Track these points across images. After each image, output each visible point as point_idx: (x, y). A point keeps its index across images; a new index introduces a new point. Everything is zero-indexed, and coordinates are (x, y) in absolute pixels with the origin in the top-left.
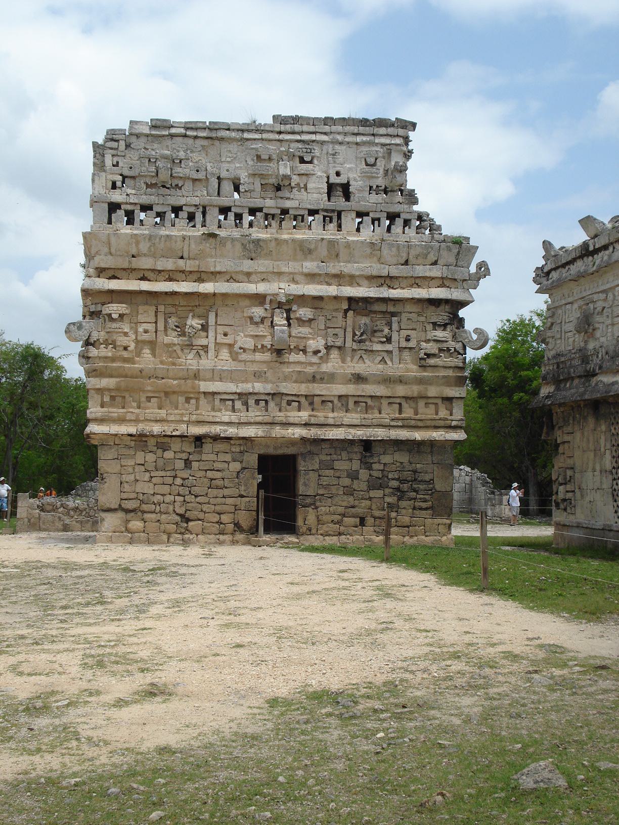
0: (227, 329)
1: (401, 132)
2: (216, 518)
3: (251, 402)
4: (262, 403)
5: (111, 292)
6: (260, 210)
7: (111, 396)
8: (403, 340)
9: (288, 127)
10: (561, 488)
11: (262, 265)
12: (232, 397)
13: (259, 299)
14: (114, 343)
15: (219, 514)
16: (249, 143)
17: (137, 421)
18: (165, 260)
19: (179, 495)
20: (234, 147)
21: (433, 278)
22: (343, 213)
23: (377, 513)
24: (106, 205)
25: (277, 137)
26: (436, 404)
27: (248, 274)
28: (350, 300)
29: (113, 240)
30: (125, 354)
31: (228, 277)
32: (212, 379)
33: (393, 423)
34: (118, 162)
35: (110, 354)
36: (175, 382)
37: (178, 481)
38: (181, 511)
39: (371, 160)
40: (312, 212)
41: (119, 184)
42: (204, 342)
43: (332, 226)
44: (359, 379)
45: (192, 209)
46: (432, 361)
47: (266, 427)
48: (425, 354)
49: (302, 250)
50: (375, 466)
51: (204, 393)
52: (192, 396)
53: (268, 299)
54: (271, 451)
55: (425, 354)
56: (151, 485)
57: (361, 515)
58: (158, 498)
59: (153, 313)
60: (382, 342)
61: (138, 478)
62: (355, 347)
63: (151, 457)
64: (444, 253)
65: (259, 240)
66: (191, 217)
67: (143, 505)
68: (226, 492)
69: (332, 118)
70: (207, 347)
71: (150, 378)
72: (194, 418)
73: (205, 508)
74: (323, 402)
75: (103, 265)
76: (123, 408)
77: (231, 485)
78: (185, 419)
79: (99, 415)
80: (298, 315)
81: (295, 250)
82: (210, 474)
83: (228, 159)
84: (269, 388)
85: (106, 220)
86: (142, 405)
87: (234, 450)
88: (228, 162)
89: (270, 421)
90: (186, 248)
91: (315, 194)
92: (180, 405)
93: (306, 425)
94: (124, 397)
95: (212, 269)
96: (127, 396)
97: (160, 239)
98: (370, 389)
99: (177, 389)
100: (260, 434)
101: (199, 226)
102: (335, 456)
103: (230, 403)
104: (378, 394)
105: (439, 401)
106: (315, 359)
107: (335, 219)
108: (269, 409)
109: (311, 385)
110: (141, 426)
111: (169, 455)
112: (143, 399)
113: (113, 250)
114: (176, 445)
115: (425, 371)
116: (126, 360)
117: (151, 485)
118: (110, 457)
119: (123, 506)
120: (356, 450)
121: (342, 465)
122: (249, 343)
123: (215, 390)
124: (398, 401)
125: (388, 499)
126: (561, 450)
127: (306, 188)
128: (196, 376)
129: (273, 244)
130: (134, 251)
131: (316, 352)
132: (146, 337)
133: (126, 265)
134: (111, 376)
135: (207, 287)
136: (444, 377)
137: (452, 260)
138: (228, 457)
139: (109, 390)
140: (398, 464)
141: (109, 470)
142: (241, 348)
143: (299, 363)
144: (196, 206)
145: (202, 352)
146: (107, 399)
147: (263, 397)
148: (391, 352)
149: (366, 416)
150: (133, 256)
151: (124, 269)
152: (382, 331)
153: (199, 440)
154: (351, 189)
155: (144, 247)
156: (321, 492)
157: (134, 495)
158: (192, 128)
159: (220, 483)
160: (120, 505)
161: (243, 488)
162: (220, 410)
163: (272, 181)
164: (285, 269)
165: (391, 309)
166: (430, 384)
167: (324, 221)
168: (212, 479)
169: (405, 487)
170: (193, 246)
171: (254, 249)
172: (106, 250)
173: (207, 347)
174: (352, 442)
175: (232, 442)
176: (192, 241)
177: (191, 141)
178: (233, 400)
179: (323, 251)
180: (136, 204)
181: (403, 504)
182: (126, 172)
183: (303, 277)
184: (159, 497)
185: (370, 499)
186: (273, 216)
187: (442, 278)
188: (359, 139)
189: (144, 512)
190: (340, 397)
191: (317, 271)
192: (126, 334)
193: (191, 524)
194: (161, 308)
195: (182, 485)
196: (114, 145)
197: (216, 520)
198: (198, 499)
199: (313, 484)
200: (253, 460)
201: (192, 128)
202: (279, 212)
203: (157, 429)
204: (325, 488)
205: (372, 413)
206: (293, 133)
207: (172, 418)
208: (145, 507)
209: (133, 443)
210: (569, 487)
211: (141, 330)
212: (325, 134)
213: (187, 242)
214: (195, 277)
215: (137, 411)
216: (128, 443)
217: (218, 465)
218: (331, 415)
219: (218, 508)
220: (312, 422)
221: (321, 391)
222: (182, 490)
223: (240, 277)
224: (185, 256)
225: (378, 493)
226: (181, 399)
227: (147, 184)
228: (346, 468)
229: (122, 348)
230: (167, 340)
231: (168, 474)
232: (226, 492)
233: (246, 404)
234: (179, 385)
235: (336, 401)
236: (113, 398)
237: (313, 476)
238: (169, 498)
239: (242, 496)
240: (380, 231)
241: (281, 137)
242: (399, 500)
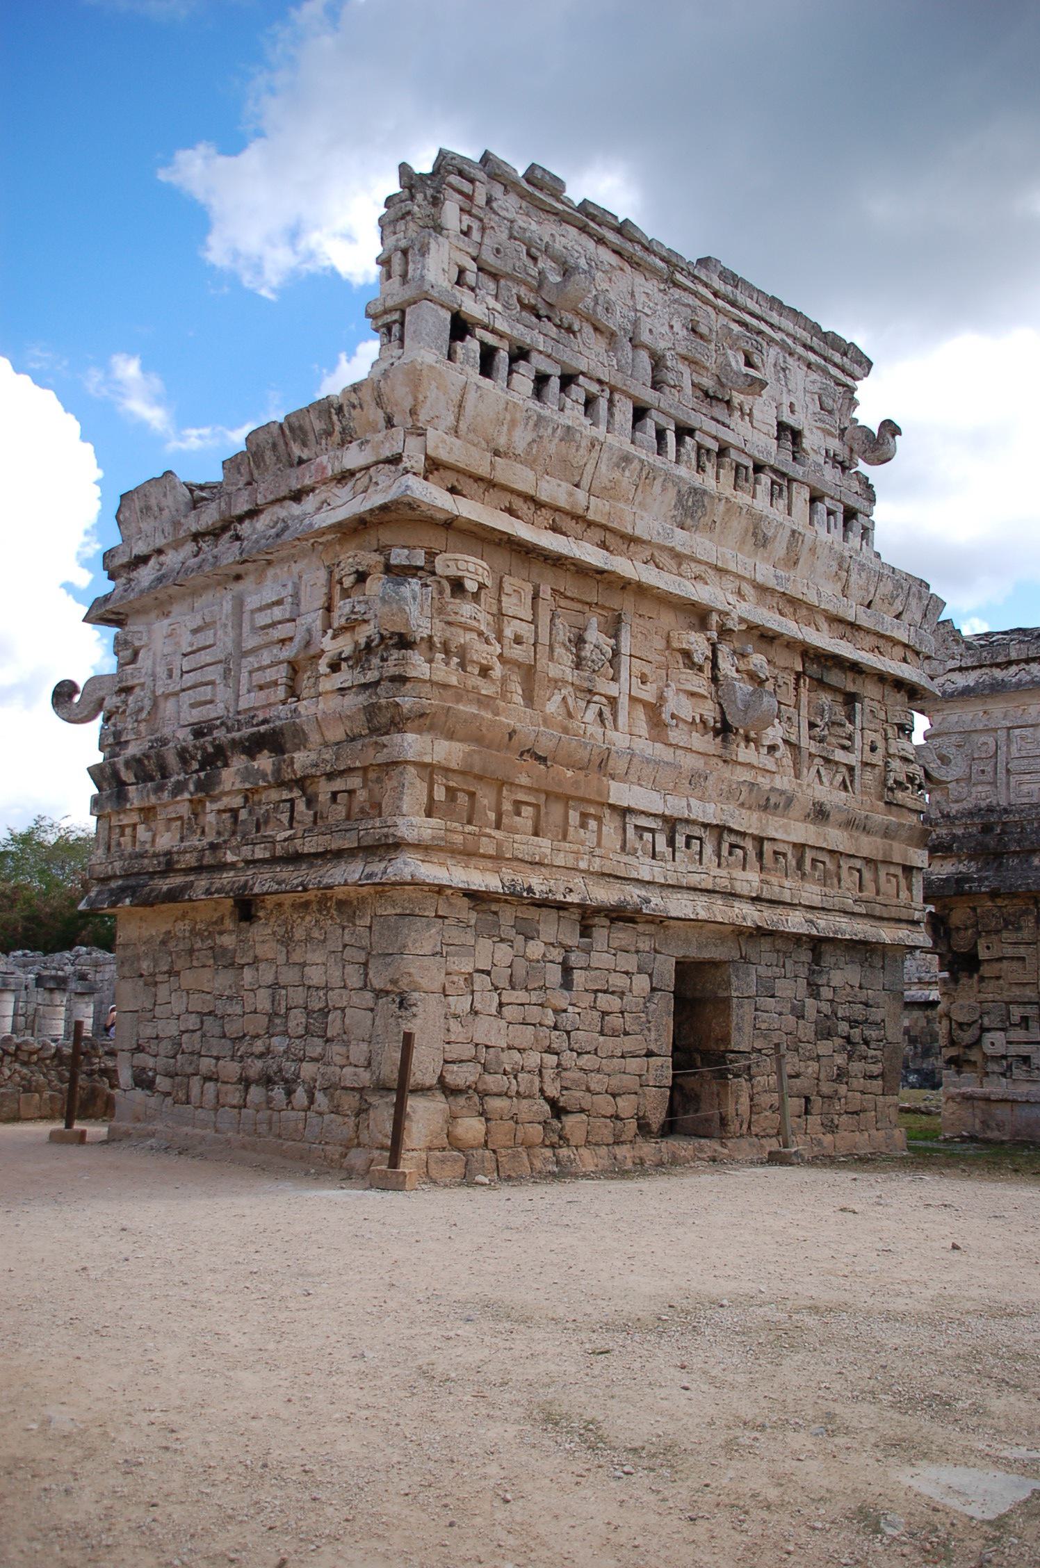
0: (647, 669)
1: (857, 371)
2: (604, 1104)
3: (680, 840)
4: (696, 844)
5: (449, 524)
6: (691, 432)
7: (448, 789)
8: (867, 748)
9: (727, 289)
10: (998, 1036)
11: (701, 544)
12: (653, 826)
13: (700, 616)
14: (462, 652)
15: (614, 1096)
16: (677, 293)
17: (498, 858)
18: (554, 481)
19: (549, 1050)
20: (652, 286)
21: (895, 642)
22: (795, 485)
23: (826, 1088)
24: (448, 316)
25: (711, 297)
26: (895, 876)
27: (679, 557)
28: (810, 654)
29: (471, 397)
30: (487, 689)
31: (647, 554)
32: (624, 778)
33: (857, 909)
34: (469, 227)
35: (453, 681)
36: (570, 774)
37: (550, 1019)
38: (552, 1091)
39: (829, 403)
40: (758, 468)
41: (470, 278)
42: (612, 689)
43: (782, 503)
44: (820, 814)
45: (594, 388)
46: (900, 796)
47: (702, 900)
48: (895, 781)
49: (755, 534)
50: (826, 993)
51: (613, 807)
52: (592, 811)
53: (715, 618)
54: (693, 953)
55: (895, 781)
56: (503, 1023)
57: (806, 1092)
58: (510, 1060)
59: (529, 601)
60: (844, 748)
61: (478, 1006)
62: (813, 751)
63: (504, 953)
64: (913, 602)
65: (705, 492)
66: (590, 402)
67: (487, 1077)
68: (628, 1044)
69: (781, 303)
70: (613, 701)
71: (522, 754)
72: (597, 865)
73: (596, 1081)
74: (776, 853)
75: (443, 455)
76: (470, 822)
77: (637, 1028)
78: (583, 865)
79: (427, 834)
80: (752, 667)
81: (747, 531)
82: (604, 1001)
83: (646, 310)
84: (709, 812)
85: (445, 352)
86: (505, 820)
87: (641, 946)
88: (647, 315)
89: (710, 887)
90: (590, 468)
91: (754, 435)
92: (571, 829)
93: (756, 900)
94: (472, 795)
95: (629, 531)
96: (479, 793)
97: (554, 430)
98: (836, 838)
99: (571, 791)
100: (703, 915)
101: (603, 427)
102: (777, 970)
103: (647, 836)
104: (841, 849)
105: (899, 871)
106: (769, 763)
107: (785, 493)
108: (705, 860)
109: (763, 815)
110: (508, 874)
111: (535, 949)
112: (507, 806)
113: (463, 427)
114: (550, 928)
115: (890, 813)
116: (484, 702)
117: (503, 1023)
118: (427, 949)
119: (449, 1078)
120: (803, 959)
121: (785, 988)
122: (687, 709)
123: (633, 805)
124: (858, 864)
125: (840, 1060)
126: (986, 970)
127: (750, 415)
128: (602, 764)
129: (721, 507)
130: (502, 441)
131: (772, 748)
132: (517, 653)
133: (483, 471)
134: (451, 736)
135: (623, 566)
136: (911, 828)
137: (918, 617)
138: (629, 962)
139: (447, 770)
140: (848, 988)
141: (424, 983)
142: (673, 716)
143: (750, 766)
144: (600, 382)
145: (607, 711)
146: (440, 794)
147: (697, 831)
148: (851, 769)
149: (827, 890)
150: (497, 453)
151: (478, 479)
152: (843, 726)
153: (587, 918)
154: (806, 443)
155: (521, 439)
156: (758, 1045)
157: (469, 1052)
158: (593, 218)
159: (615, 1021)
160: (441, 1079)
161: (653, 1035)
162: (634, 852)
163: (708, 382)
164: (732, 567)
165: (851, 688)
166: (893, 839)
167: (772, 495)
168: (605, 1014)
169: (856, 1032)
170: (603, 468)
171: (692, 507)
172: (450, 420)
173: (613, 701)
174: (797, 939)
175: (641, 928)
176: (605, 456)
177: (591, 244)
178: (652, 831)
179: (779, 548)
180: (501, 335)
181: (856, 1067)
182: (488, 257)
183: (752, 591)
184: (516, 1055)
185: (818, 1058)
186: (708, 451)
187: (906, 646)
188: (812, 357)
189: (483, 1095)
190: (795, 845)
191: (772, 583)
192: (480, 634)
193: (569, 1120)
194: (546, 591)
195: (555, 1028)
196: (466, 187)
197: (610, 1111)
198: (585, 1061)
199: (748, 1029)
200: (666, 968)
201: (593, 218)
202: (715, 446)
203: (538, 883)
204: (765, 1037)
205: (832, 886)
206: (733, 304)
207: (560, 860)
208: (493, 1082)
209: (473, 917)
210: (1018, 1034)
211: (508, 632)
212: (772, 326)
213: (595, 454)
214: (598, 535)
215: (498, 834)
216: (464, 915)
217: (618, 981)
218: (787, 884)
219: (615, 1082)
220: (765, 895)
221: (776, 830)
222: (558, 1039)
223: (664, 559)
224: (585, 483)
225: (824, 1048)
226: (574, 817)
227: (519, 300)
228: (790, 993)
229: (476, 671)
230: (554, 671)
231: (535, 997)
232: (628, 1044)
233: (671, 842)
234: (576, 783)
235: (789, 850)
236: (451, 792)
237: (748, 1008)
238: (533, 1059)
239: (650, 1054)
240: (837, 533)
241: (720, 303)
242: (850, 1058)
